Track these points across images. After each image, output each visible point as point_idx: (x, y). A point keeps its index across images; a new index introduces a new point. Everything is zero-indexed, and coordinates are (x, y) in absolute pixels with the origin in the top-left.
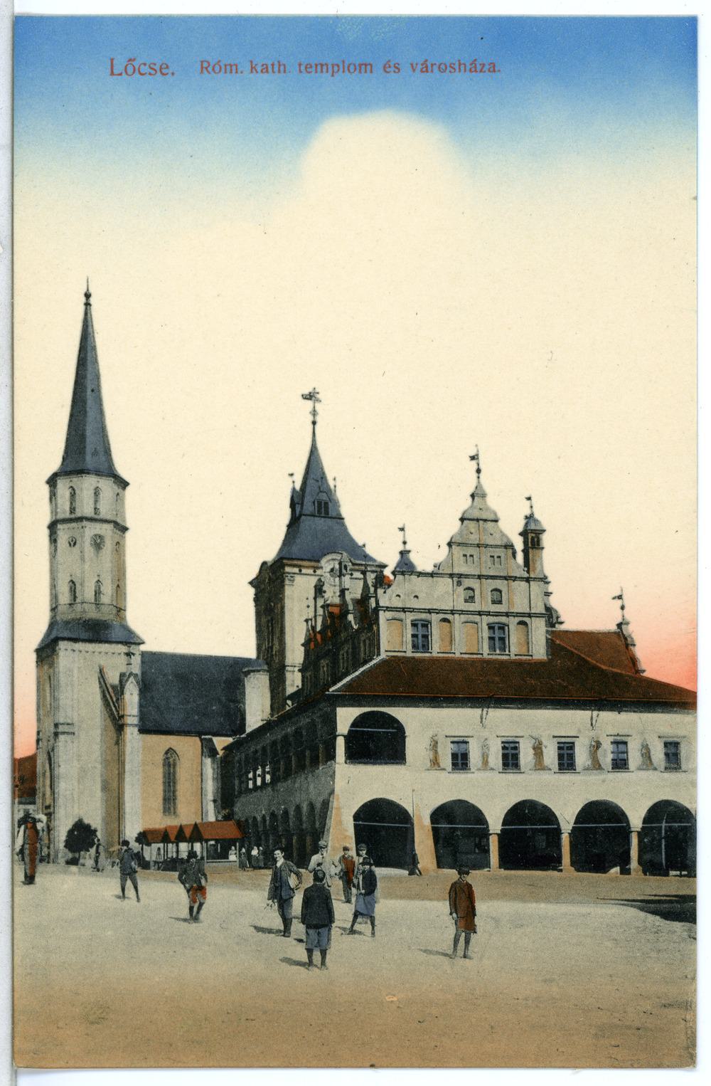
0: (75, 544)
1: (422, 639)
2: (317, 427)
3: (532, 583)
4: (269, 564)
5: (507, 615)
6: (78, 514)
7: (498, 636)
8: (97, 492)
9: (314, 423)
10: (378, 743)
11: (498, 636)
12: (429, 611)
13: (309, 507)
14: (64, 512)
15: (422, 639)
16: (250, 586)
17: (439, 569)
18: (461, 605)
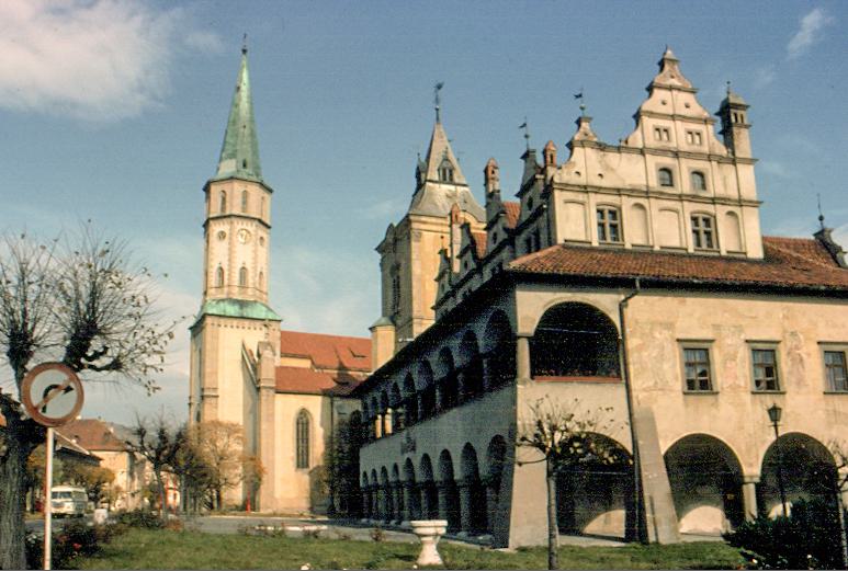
0: (224, 237)
1: (611, 222)
2: (440, 113)
3: (739, 166)
4: (395, 225)
5: (714, 201)
6: (228, 213)
7: (704, 228)
8: (245, 194)
9: (437, 109)
10: (583, 347)
11: (704, 228)
12: (619, 192)
13: (433, 174)
14: (216, 212)
15: (611, 222)
16: (376, 253)
17: (626, 142)
18: (654, 183)
